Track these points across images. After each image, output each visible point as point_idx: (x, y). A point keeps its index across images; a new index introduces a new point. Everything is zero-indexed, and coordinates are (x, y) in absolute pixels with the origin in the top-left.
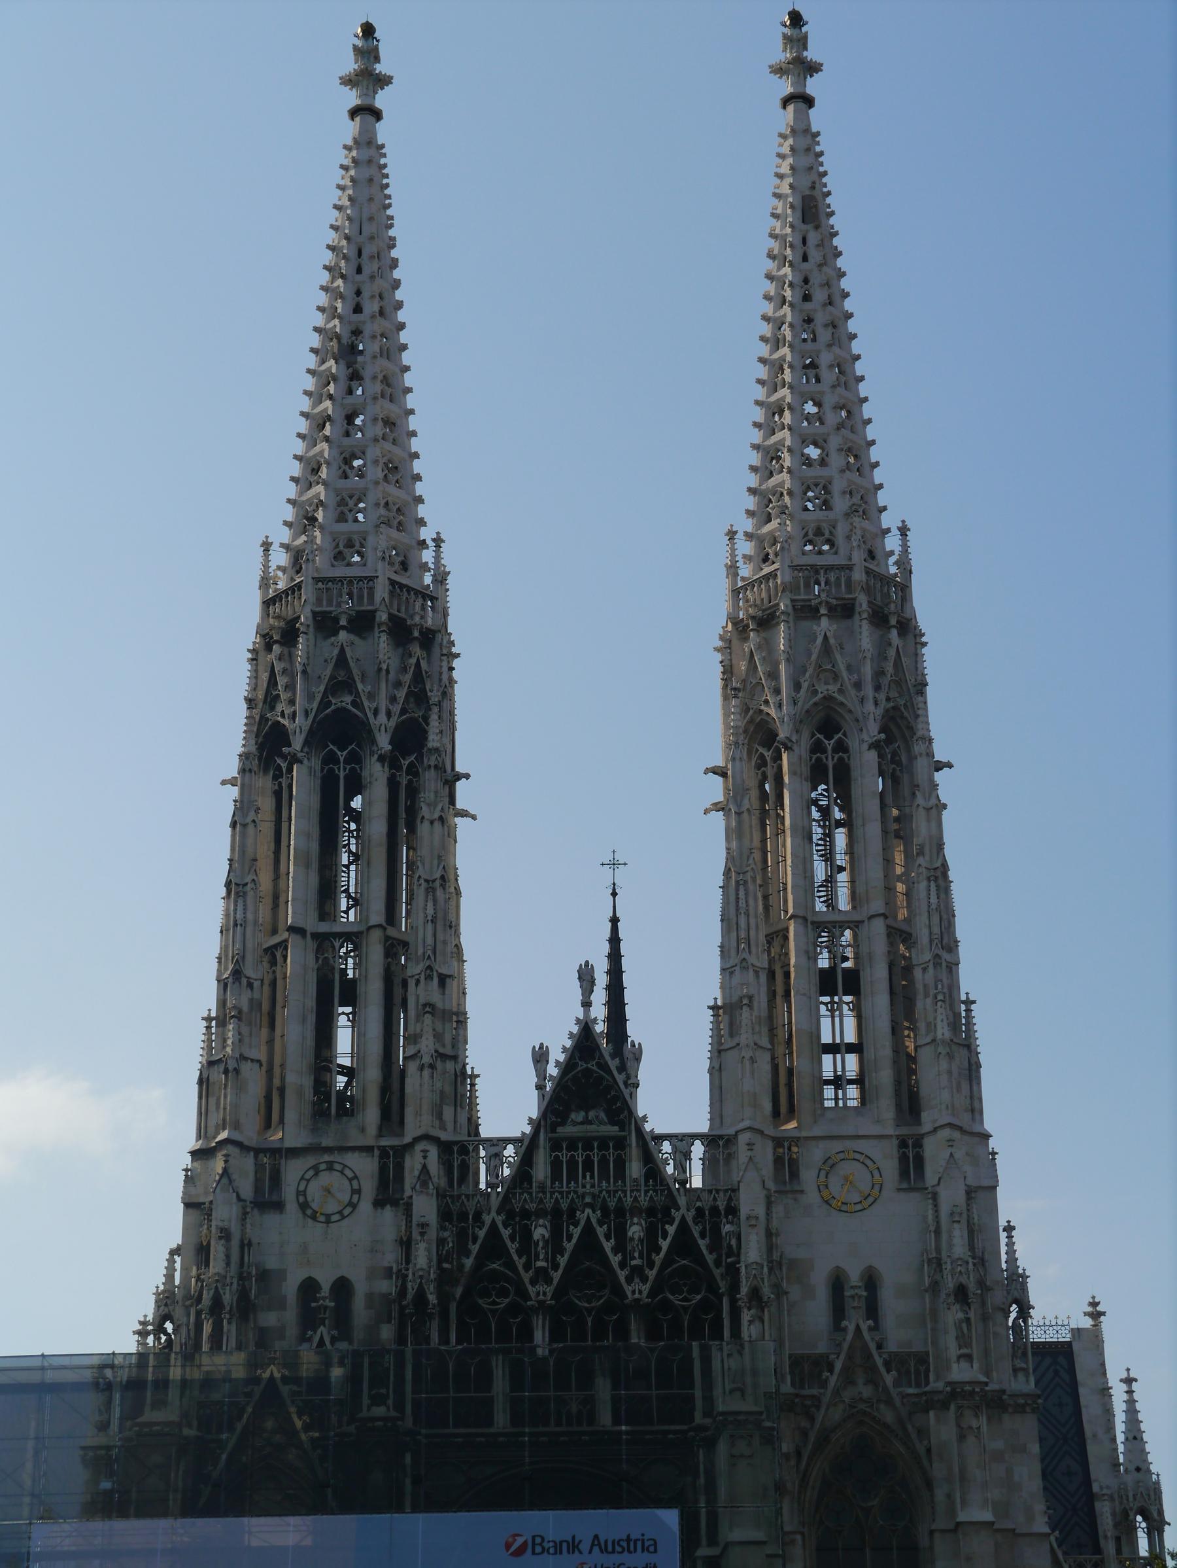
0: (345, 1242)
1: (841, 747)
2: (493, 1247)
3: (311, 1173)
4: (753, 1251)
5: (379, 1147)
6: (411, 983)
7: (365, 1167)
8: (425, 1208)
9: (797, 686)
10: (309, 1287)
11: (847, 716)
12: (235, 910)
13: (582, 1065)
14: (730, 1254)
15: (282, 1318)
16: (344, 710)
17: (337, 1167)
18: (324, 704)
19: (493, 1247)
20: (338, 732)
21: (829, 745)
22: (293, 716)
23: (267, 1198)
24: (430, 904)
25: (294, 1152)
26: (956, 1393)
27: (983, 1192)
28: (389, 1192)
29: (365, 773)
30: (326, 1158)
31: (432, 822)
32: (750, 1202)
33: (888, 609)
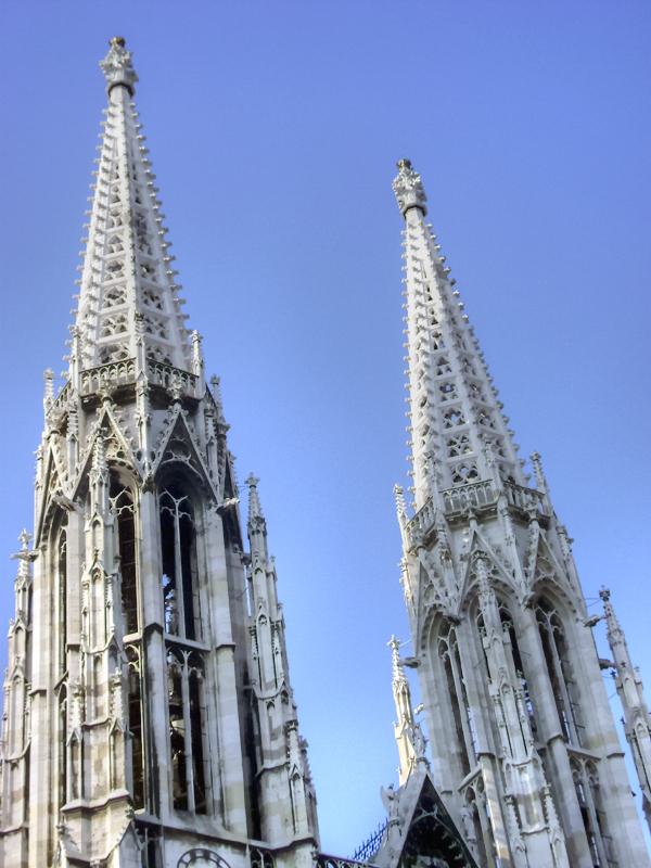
1: (554, 621)
3: (187, 858)
5: (251, 847)
6: (262, 706)
9: (526, 564)
11: (561, 599)
12: (106, 594)
13: (425, 814)
16: (183, 464)
17: (212, 856)
18: (167, 456)
21: (549, 616)
22: (139, 456)
24: (276, 640)
25: (172, 833)
29: (198, 523)
30: (202, 846)
31: (267, 575)
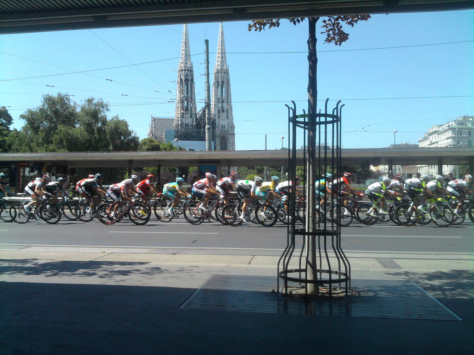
0: (188, 121)
2: (199, 122)
4: (217, 124)
7: (190, 115)
8: (194, 119)
10: (186, 124)
14: (215, 123)
15: (184, 126)
19: (199, 122)
20: (187, 80)
23: (182, 117)
26: (230, 134)
27: (232, 120)
28: (191, 117)
32: (217, 120)
33: (227, 72)
